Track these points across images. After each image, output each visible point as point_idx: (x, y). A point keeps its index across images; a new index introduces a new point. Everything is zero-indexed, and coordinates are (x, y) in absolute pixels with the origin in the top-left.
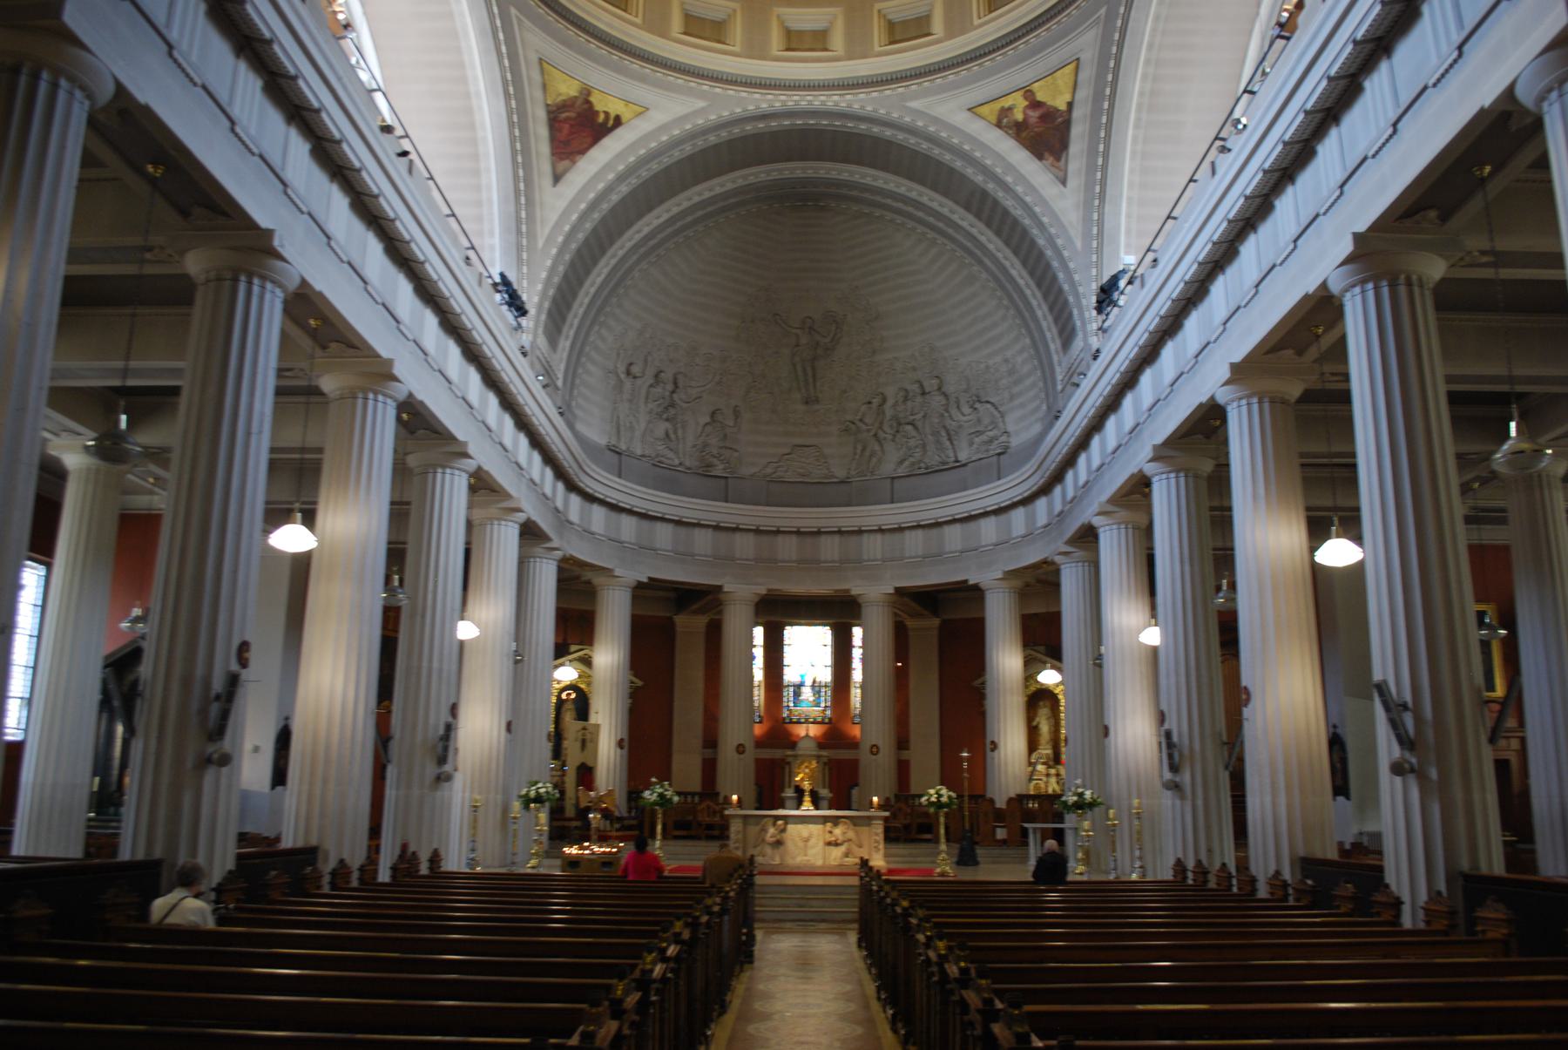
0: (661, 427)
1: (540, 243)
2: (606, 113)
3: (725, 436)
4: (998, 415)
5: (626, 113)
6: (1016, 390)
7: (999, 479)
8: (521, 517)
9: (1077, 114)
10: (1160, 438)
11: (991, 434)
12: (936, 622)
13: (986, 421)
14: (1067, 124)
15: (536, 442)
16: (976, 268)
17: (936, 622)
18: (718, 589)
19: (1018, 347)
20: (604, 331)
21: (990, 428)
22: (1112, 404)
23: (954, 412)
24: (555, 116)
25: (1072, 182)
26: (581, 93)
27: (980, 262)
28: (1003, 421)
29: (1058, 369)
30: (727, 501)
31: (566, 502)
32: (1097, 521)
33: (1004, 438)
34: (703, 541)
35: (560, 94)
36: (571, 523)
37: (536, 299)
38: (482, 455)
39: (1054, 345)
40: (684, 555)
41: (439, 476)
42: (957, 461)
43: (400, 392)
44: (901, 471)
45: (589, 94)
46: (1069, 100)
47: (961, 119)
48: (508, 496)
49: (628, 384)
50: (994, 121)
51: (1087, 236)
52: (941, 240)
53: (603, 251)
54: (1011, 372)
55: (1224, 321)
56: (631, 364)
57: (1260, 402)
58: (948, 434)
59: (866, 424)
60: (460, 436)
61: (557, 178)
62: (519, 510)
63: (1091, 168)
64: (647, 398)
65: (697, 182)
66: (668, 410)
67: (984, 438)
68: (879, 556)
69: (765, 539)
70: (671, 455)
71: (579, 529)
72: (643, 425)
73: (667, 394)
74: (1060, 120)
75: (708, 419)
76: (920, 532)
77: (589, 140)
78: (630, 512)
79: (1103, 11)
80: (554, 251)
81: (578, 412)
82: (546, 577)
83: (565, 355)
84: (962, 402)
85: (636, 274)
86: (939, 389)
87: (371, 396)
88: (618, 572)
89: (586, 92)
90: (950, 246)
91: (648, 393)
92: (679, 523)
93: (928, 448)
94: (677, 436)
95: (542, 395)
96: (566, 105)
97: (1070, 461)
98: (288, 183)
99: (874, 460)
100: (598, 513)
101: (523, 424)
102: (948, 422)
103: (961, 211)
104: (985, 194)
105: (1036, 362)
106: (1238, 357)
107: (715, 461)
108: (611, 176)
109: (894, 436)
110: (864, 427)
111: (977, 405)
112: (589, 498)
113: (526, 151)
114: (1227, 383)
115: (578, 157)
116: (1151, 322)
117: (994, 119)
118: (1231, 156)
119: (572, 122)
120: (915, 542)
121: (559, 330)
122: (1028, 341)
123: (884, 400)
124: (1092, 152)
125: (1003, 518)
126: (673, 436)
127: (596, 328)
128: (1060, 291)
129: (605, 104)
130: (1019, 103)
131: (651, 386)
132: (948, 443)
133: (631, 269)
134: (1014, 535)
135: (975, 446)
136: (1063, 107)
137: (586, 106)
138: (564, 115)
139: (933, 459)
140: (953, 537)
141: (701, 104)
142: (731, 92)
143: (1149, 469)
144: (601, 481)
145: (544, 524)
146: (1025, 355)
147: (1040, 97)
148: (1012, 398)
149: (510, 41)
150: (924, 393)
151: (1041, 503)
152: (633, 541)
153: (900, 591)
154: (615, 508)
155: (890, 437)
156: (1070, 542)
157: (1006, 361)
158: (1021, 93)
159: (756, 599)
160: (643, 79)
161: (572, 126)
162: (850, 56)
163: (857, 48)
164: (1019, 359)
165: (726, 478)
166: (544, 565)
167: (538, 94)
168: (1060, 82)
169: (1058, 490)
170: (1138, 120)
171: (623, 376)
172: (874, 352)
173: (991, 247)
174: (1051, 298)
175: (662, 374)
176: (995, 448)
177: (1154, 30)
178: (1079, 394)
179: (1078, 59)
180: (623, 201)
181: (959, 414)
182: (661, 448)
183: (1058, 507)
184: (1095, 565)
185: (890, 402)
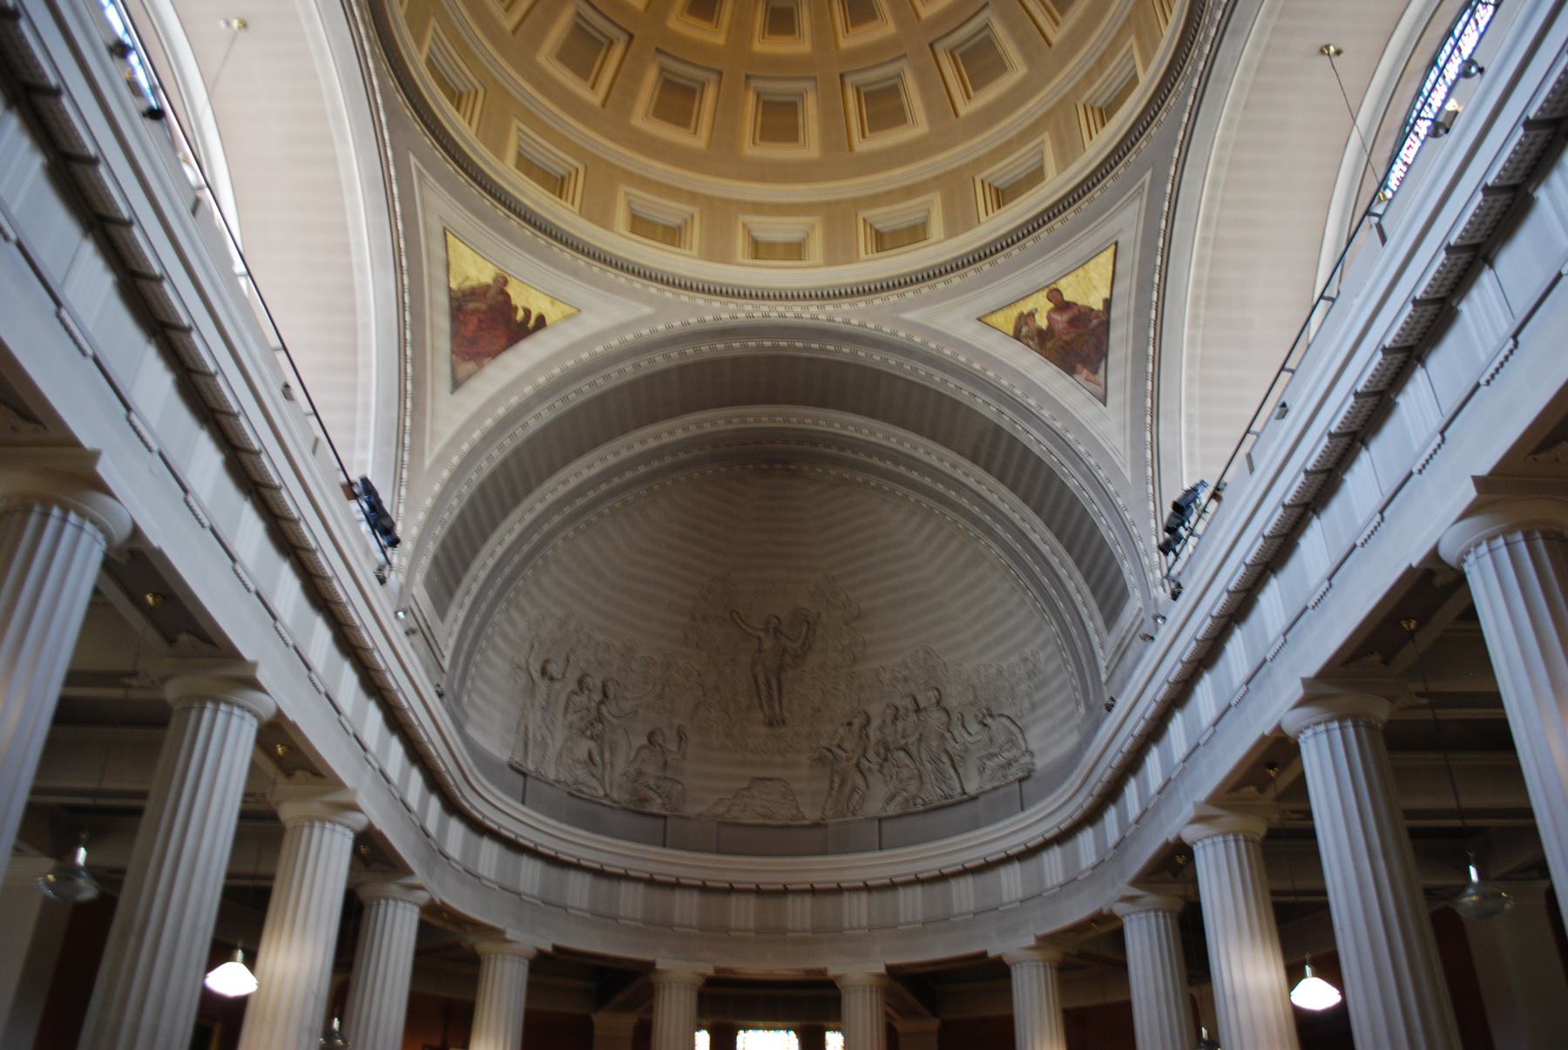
0: (585, 746)
2: (528, 312)
3: (666, 763)
4: (1016, 730)
5: (552, 315)
6: (1038, 696)
7: (1022, 809)
8: (359, 821)
9: (1115, 313)
10: (1312, 667)
11: (1008, 755)
12: (934, 1024)
13: (1001, 738)
14: (1105, 325)
15: (396, 720)
16: (986, 540)
17: (934, 1024)
18: (650, 966)
19: (1040, 639)
20: (515, 614)
21: (1006, 747)
22: (1209, 653)
23: (958, 731)
24: (461, 303)
25: (1112, 399)
26: (495, 280)
27: (990, 532)
28: (1024, 739)
29: (1100, 653)
30: (664, 846)
31: (442, 828)
32: (1189, 834)
33: (1026, 759)
34: (631, 899)
35: (467, 278)
36: (447, 858)
37: (415, 531)
39: (1094, 623)
40: (604, 918)
41: (207, 715)
42: (964, 793)
44: (892, 810)
45: (506, 282)
46: (1108, 296)
47: (968, 331)
48: (338, 785)
49: (542, 685)
50: (1011, 332)
51: (1138, 462)
52: (938, 509)
53: (517, 501)
54: (1031, 675)
55: (1379, 508)
56: (547, 661)
57: (1529, 539)
58: (952, 760)
59: (846, 751)
60: (248, 653)
61: (457, 384)
62: (354, 808)
63: (1138, 376)
64: (566, 708)
65: (639, 425)
66: (594, 725)
67: (1000, 760)
68: (864, 923)
69: (714, 900)
70: (594, 783)
71: (460, 868)
72: (558, 745)
73: (593, 704)
74: (1095, 322)
75: (644, 741)
76: (918, 890)
77: (503, 341)
78: (534, 853)
79: (1148, 176)
80: (445, 474)
81: (472, 713)
83: (456, 628)
84: (969, 717)
85: (558, 541)
86: (938, 703)
87: (56, 512)
88: (510, 935)
89: (502, 281)
90: (951, 515)
91: (569, 700)
92: (599, 873)
93: (925, 779)
94: (603, 760)
97: (1133, 763)
98: (237, 558)
99: (857, 796)
100: (489, 852)
102: (951, 745)
103: (966, 463)
104: (998, 430)
105: (1067, 655)
106: (1484, 467)
107: (651, 794)
108: (528, 390)
109: (881, 766)
110: (843, 755)
111: (989, 721)
112: (477, 827)
113: (419, 344)
115: (486, 361)
117: (1010, 329)
119: (481, 316)
120: (912, 903)
121: (451, 594)
122: (1055, 628)
123: (868, 720)
124: (1139, 356)
125: (1031, 864)
126: (597, 759)
127: (503, 605)
128: (1103, 542)
129: (526, 298)
130: (1041, 307)
131: (573, 693)
132: (951, 771)
133: (552, 534)
134: (1048, 884)
135: (988, 772)
136: (1098, 305)
137: (501, 298)
138: (471, 306)
139: (933, 793)
140: (964, 893)
141: (647, 310)
142: (685, 297)
146: (1050, 648)
147: (1068, 297)
148: (1034, 707)
149: (407, 197)
150: (918, 710)
151: (1086, 838)
152: (536, 892)
153: (891, 970)
154: (512, 845)
155: (875, 767)
157: (1025, 660)
158: (1045, 293)
159: (700, 981)
160: (575, 273)
161: (480, 321)
163: (838, 253)
164: (1042, 656)
165: (665, 817)
166: (400, 911)
167: (440, 273)
168: (1093, 275)
169: (1111, 815)
170: (1195, 317)
171: (536, 676)
172: (855, 660)
173: (1004, 508)
174: (1087, 562)
175: (589, 679)
176: (1015, 772)
177: (1211, 199)
178: (1153, 652)
179: (1116, 244)
180: (544, 431)
181: (965, 735)
182: (581, 773)
185: (876, 722)
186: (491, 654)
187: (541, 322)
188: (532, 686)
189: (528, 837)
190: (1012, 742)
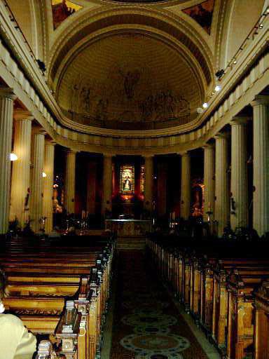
1: (50, 48)
10: (234, 115)
13: (183, 105)
15: (49, 110)
32: (215, 137)
34: (96, 140)
39: (205, 83)
43: (14, 97)
47: (180, 13)
61: (55, 29)
66: (87, 100)
78: (75, 131)
80: (54, 51)
82: (51, 149)
95: (51, 96)
96: (58, 5)
100: (66, 132)
101: (46, 105)
102: (172, 105)
116: (233, 81)
118: (258, 35)
143: (231, 123)
144: (68, 122)
145: (51, 135)
151: (199, 131)
154: (71, 130)
156: (207, 143)
169: (204, 128)
183: (204, 132)
184: (214, 149)
186: (64, 86)
187: (74, 11)
188: (72, 92)
189: (74, 127)
190: (186, 106)
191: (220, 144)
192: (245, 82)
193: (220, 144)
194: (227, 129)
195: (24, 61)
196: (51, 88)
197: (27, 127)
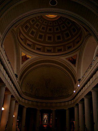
1: (20, 70)
8: (16, 100)
9: (77, 60)
10: (85, 95)
14: (76, 61)
31: (20, 98)
38: (13, 94)
47: (65, 59)
48: (14, 97)
61: (22, 64)
82: (17, 106)
95: (19, 87)
96: (24, 56)
114: (92, 90)
118: (92, 67)
129: (28, 56)
143: (84, 98)
144: (24, 96)
145: (18, 101)
162: (53, 53)
163: (54, 52)
169: (74, 99)
183: (74, 101)
184: (78, 107)
187: (29, 58)
191: (80, 106)
192: (88, 83)
193: (80, 106)
194: (83, 100)
195: (10, 74)
196: (19, 84)
197: (9, 97)
